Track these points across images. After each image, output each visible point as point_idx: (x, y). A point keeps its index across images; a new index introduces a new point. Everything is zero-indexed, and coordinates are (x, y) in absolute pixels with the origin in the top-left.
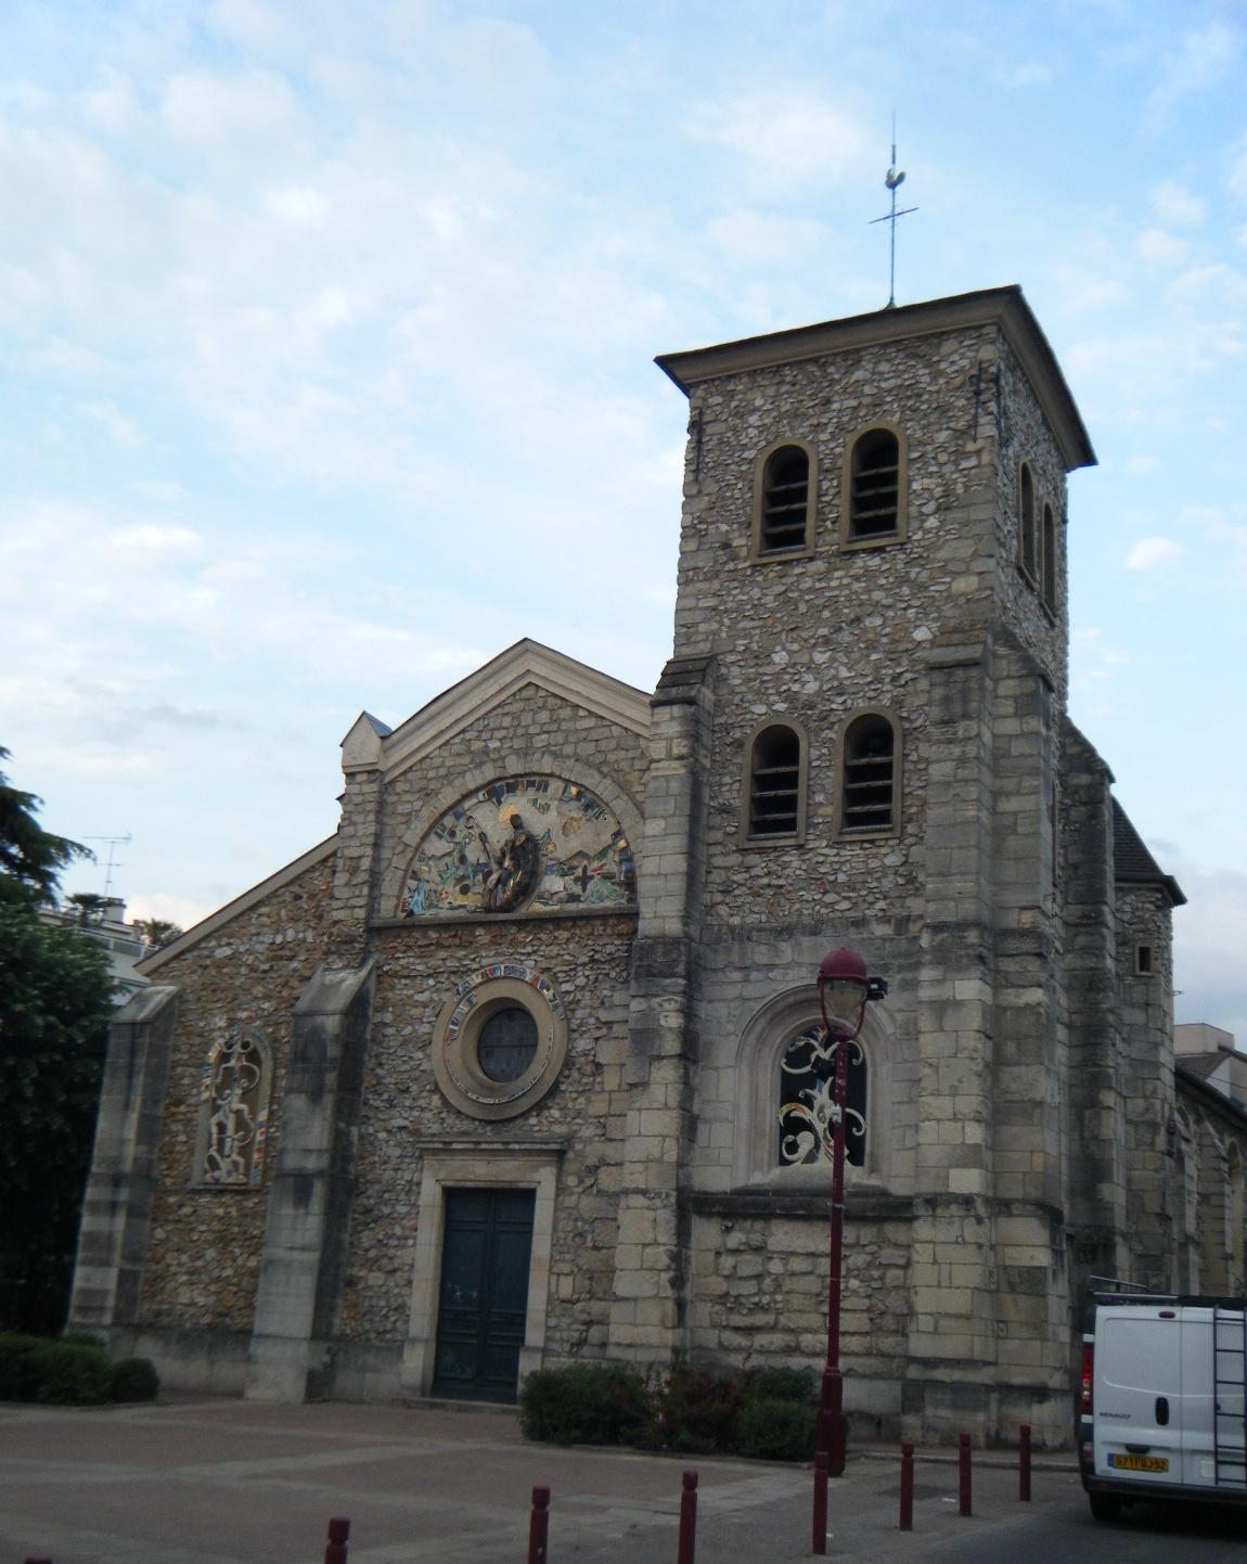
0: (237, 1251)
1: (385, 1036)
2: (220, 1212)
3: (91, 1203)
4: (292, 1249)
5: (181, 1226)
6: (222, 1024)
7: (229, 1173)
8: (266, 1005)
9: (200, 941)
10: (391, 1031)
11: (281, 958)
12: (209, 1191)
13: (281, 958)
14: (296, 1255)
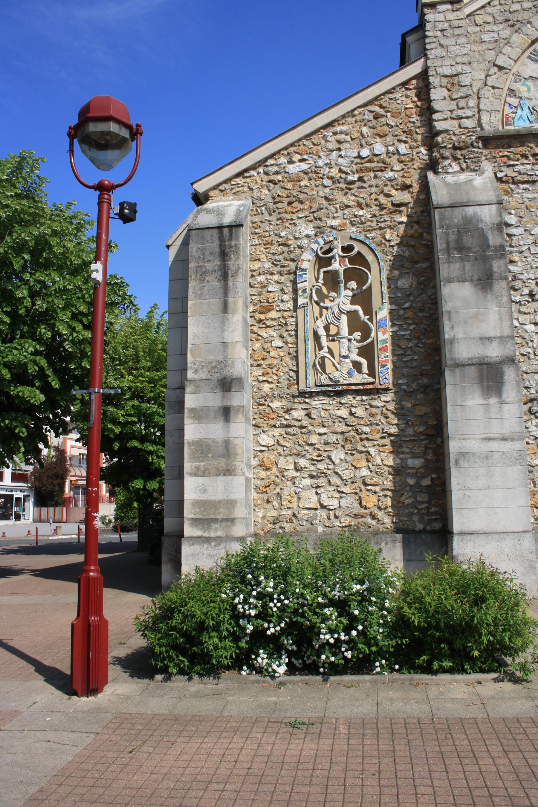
0: (372, 451)
1: (509, 235)
2: (344, 413)
3: (193, 410)
4: (490, 439)
5: (289, 430)
6: (311, 232)
7: (350, 374)
8: (361, 213)
9: (266, 159)
10: (520, 231)
11: (369, 170)
12: (325, 394)
13: (369, 170)
14: (496, 446)
